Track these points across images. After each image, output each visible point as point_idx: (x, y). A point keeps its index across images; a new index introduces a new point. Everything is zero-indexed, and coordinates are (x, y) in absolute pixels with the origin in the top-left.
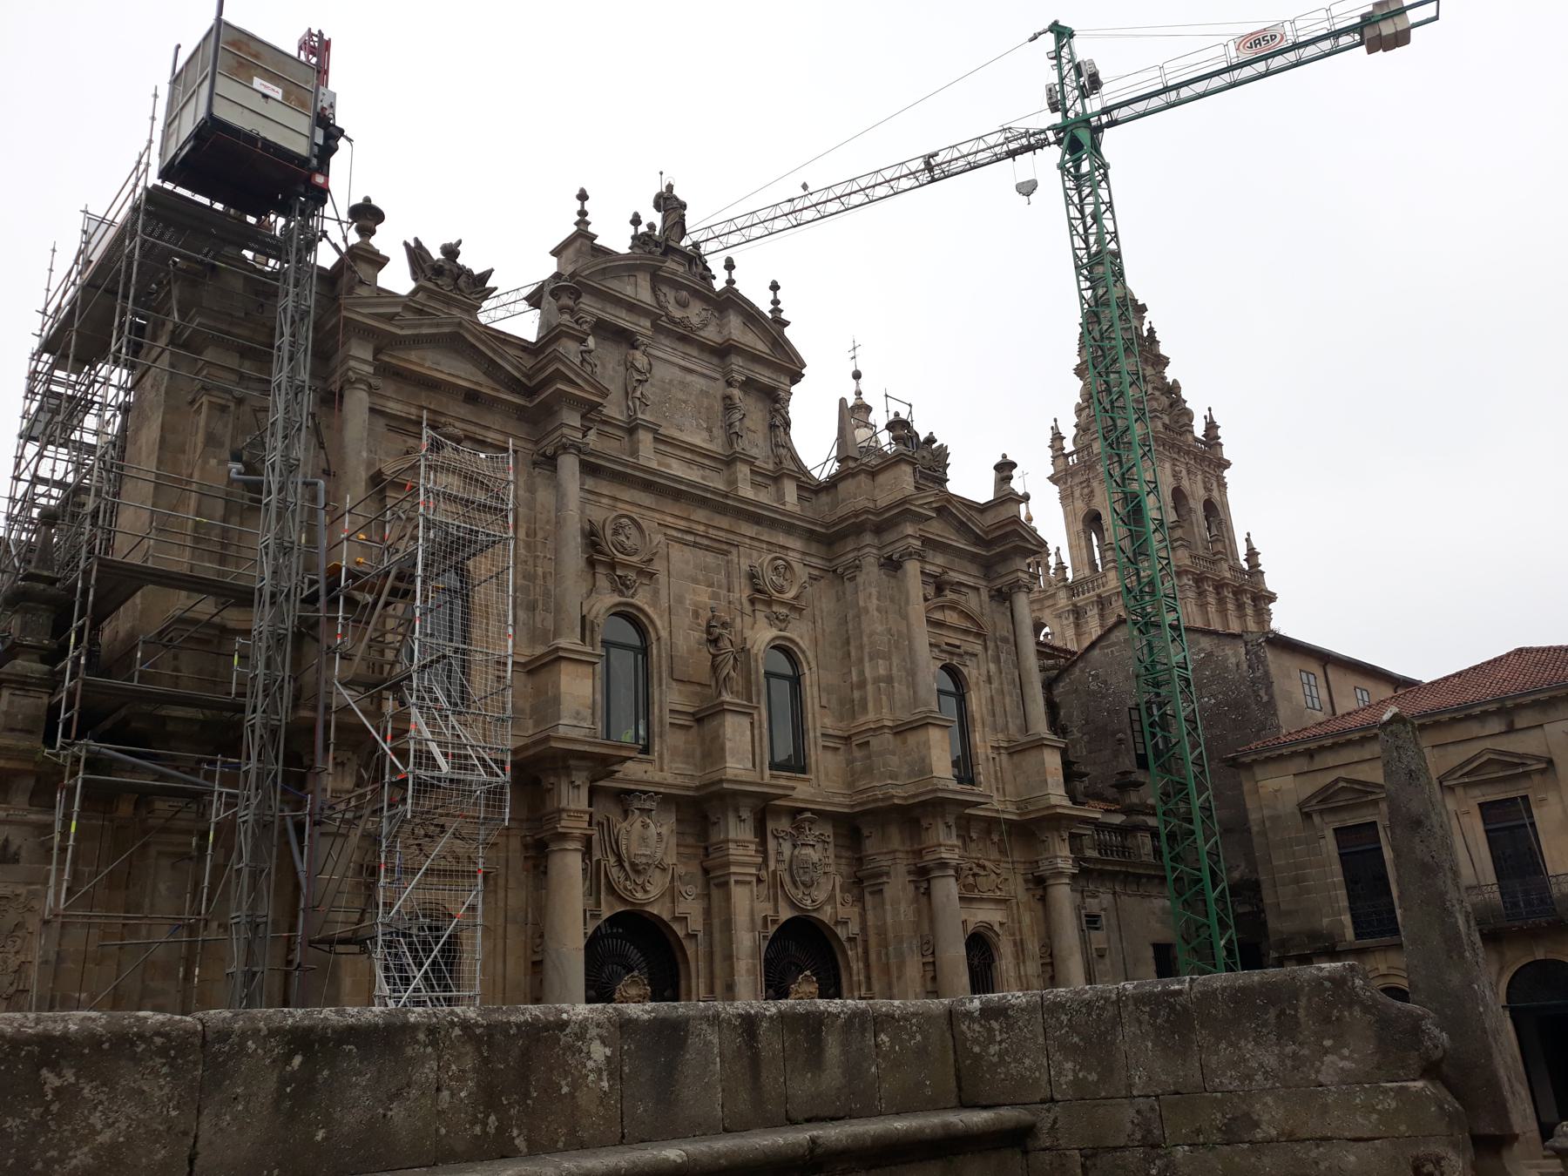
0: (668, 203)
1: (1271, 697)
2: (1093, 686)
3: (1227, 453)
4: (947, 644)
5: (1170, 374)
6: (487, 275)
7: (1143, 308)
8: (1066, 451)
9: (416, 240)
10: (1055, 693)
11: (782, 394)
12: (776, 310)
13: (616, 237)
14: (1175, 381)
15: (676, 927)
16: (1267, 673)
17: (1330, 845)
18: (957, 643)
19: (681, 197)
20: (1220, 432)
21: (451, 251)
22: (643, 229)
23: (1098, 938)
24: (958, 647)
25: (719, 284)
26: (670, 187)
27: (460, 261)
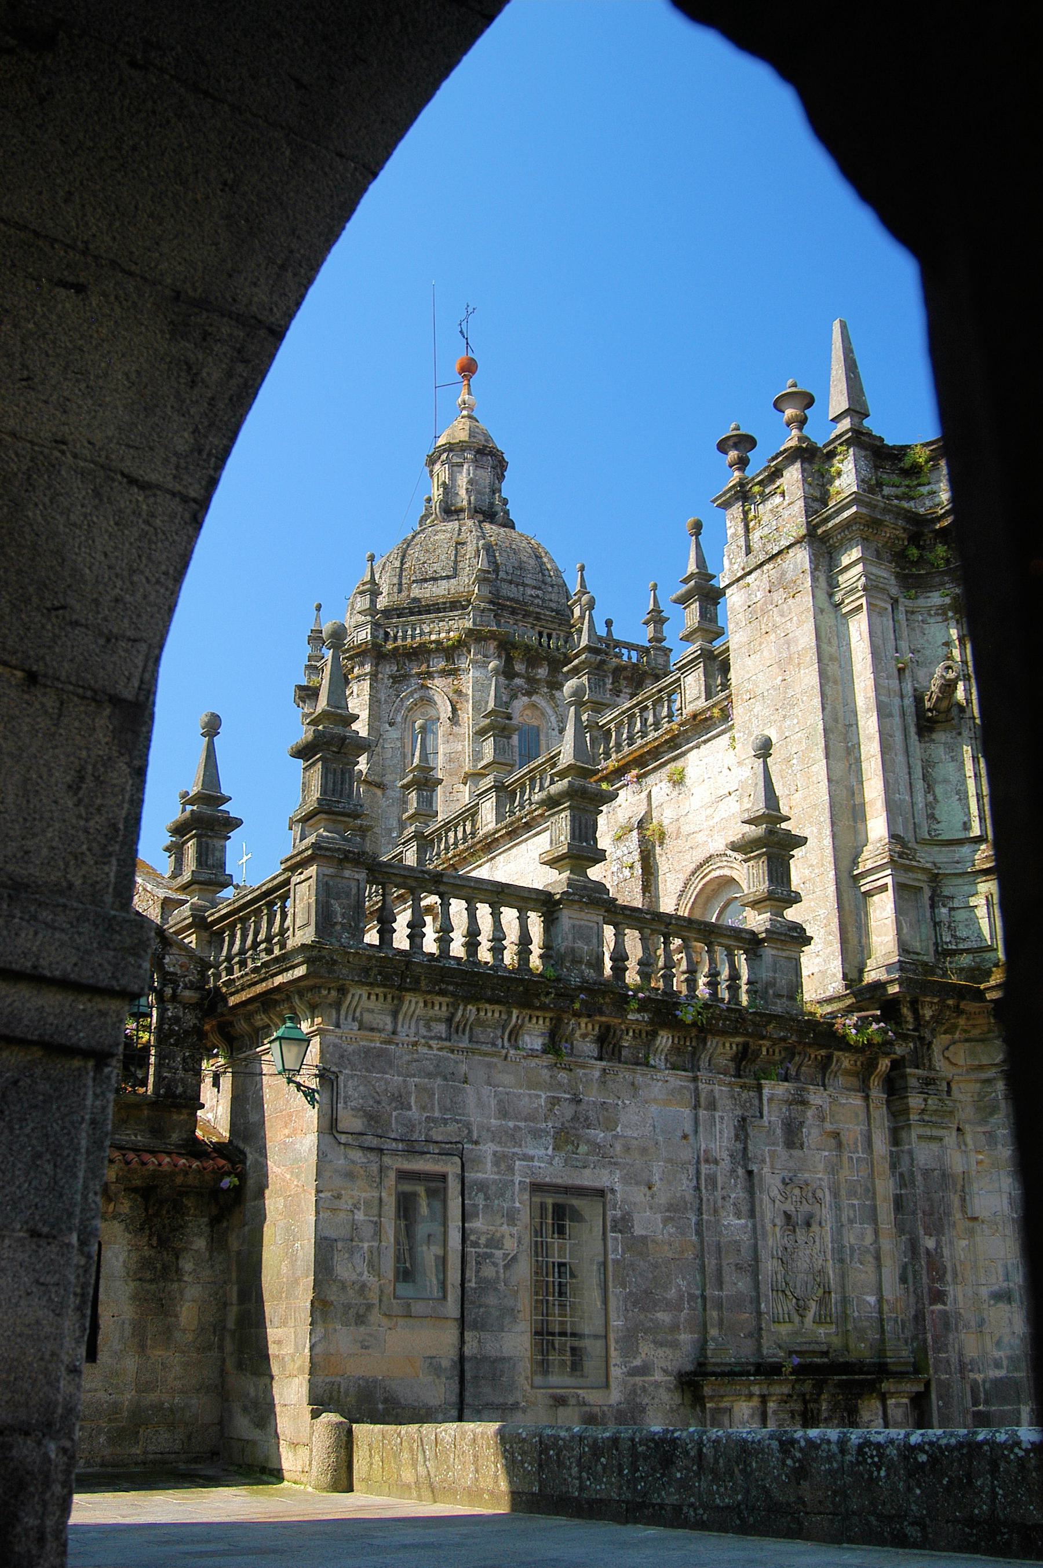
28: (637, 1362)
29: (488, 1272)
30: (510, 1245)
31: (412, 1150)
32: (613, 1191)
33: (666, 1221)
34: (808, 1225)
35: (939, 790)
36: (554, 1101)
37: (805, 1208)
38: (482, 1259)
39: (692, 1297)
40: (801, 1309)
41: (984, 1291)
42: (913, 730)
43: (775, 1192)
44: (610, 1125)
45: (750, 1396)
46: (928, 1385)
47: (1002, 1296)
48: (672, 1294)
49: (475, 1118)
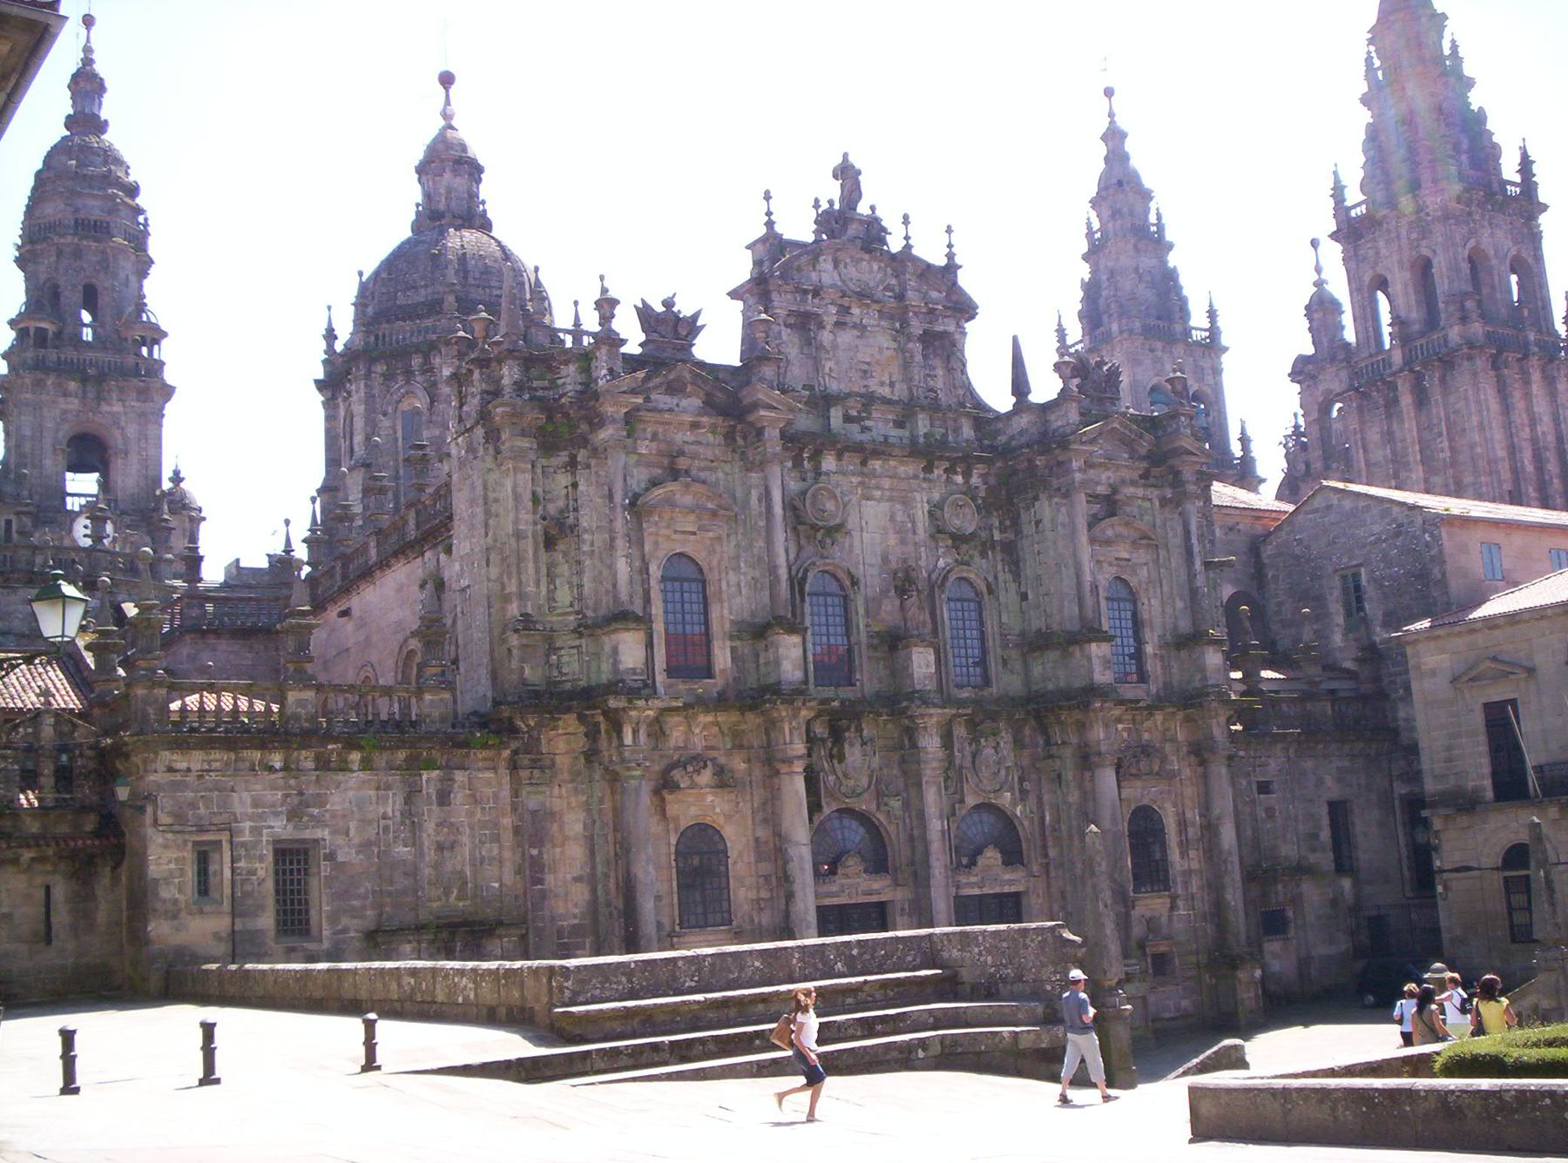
0: (847, 174)
1: (1444, 575)
2: (1297, 551)
3: (1543, 196)
4: (1117, 559)
5: (1476, 99)
6: (696, 316)
7: (1444, 17)
8: (1348, 203)
9: (643, 301)
10: (1264, 556)
11: (957, 336)
12: (950, 256)
13: (799, 227)
14: (1481, 108)
15: (881, 817)
16: (1441, 552)
17: (1478, 720)
18: (1126, 556)
19: (857, 166)
20: (1535, 169)
21: (669, 304)
22: (824, 206)
23: (1271, 799)
24: (1129, 560)
25: (895, 244)
26: (845, 156)
27: (675, 309)
28: (340, 927)
29: (248, 888)
30: (261, 873)
31: (201, 830)
32: (324, 840)
33: (358, 853)
34: (452, 847)
35: (558, 582)
36: (286, 796)
37: (452, 837)
38: (244, 882)
39: (374, 892)
40: (447, 893)
41: (569, 877)
42: (542, 545)
43: (431, 831)
44: (322, 804)
45: (410, 942)
46: (527, 929)
47: (577, 879)
48: (362, 890)
49: (238, 810)
